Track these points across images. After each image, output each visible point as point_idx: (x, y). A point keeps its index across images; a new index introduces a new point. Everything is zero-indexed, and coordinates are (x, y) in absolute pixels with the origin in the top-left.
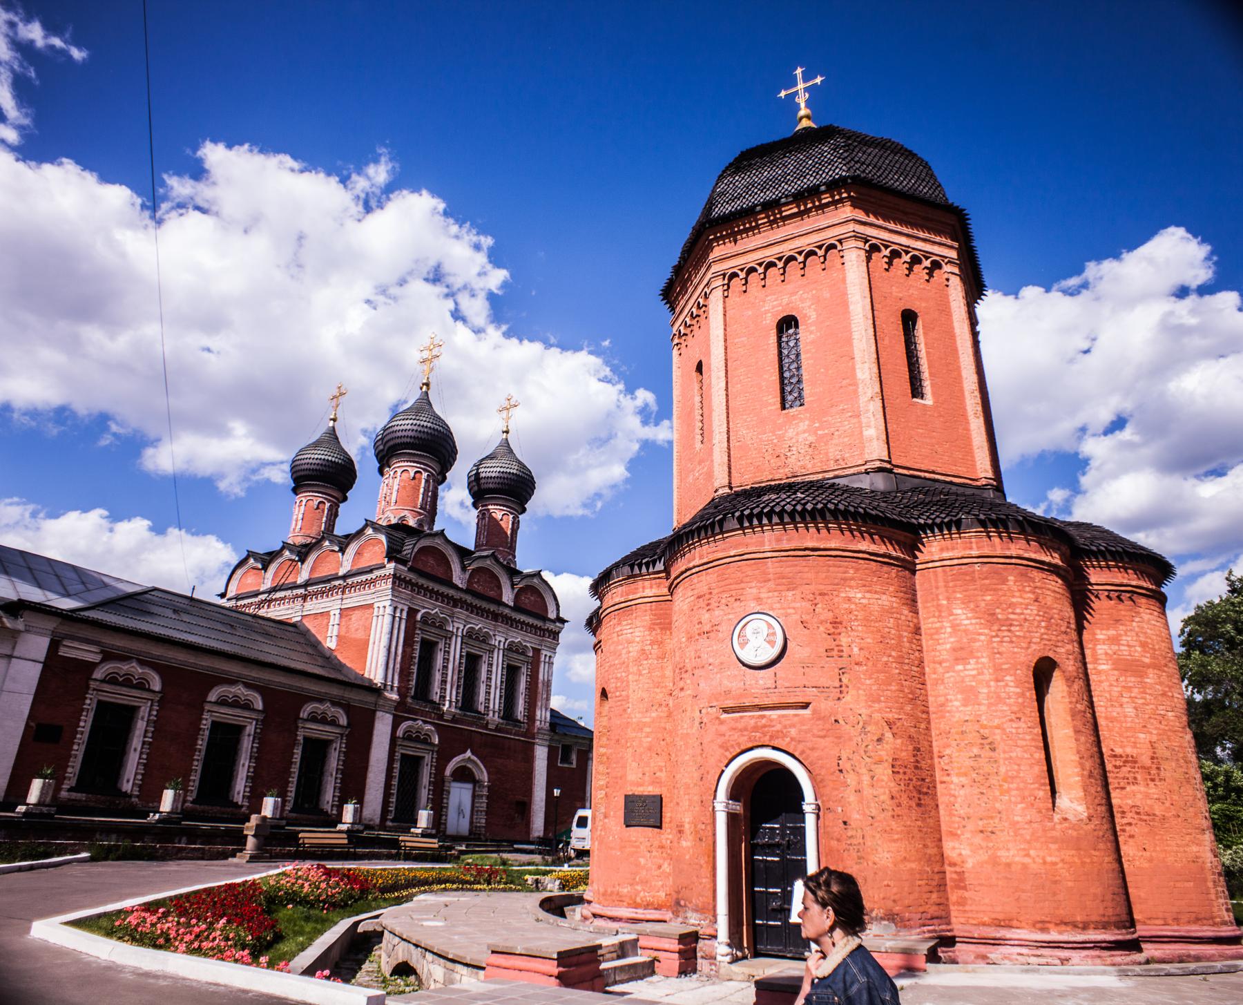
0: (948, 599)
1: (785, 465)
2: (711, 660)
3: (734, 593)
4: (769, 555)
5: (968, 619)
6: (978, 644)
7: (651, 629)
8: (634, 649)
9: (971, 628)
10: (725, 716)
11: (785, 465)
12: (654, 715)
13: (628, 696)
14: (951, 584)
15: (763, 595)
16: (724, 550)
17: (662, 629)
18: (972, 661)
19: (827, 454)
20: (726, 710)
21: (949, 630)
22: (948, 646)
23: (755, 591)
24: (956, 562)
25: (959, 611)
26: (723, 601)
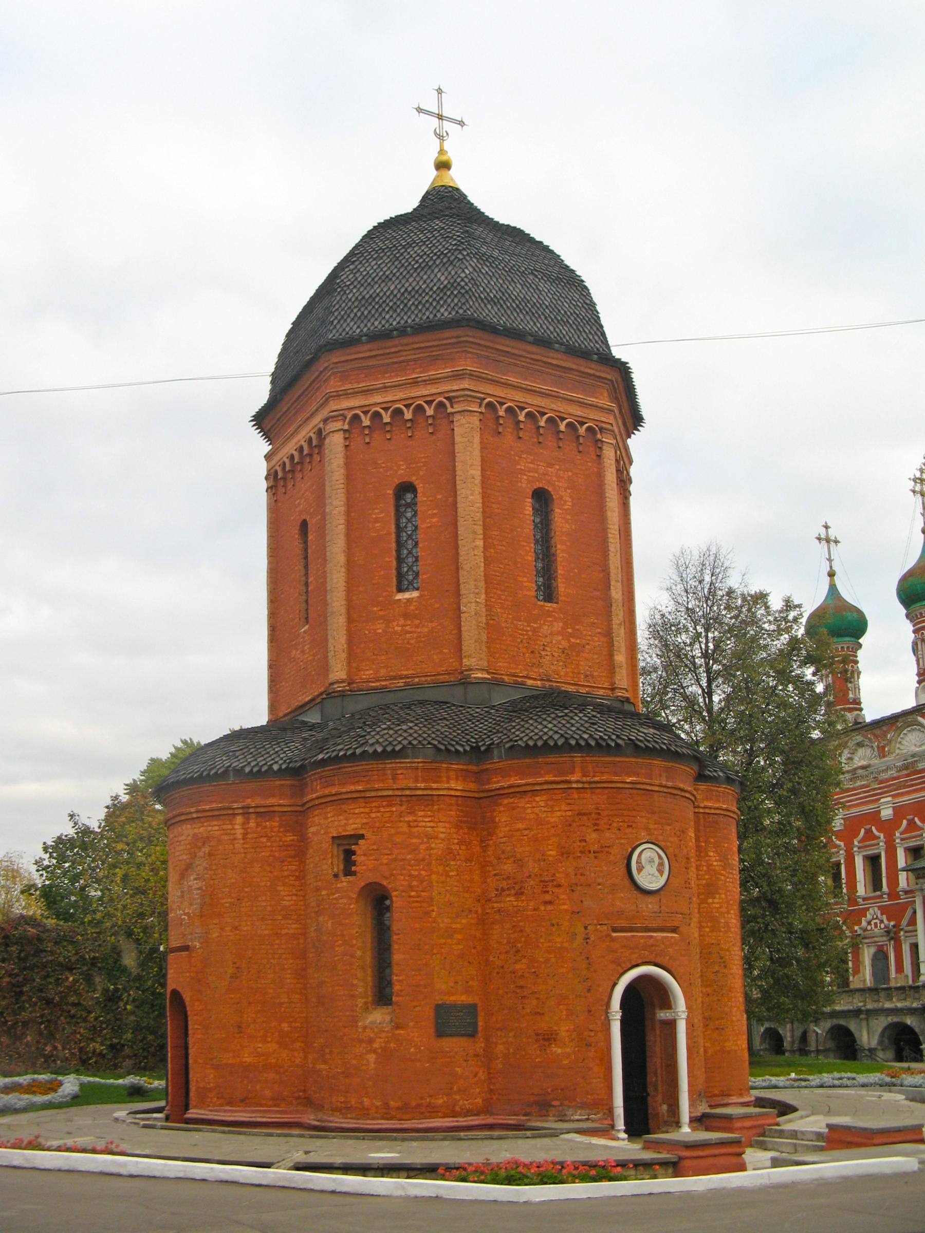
0: (705, 842)
1: (540, 665)
2: (600, 880)
3: (626, 819)
4: (656, 788)
5: (716, 861)
6: (720, 883)
7: (457, 827)
8: (438, 847)
9: (717, 868)
10: (615, 934)
11: (540, 665)
12: (464, 921)
13: (431, 899)
14: (708, 830)
15: (651, 826)
16: (616, 774)
17: (469, 828)
18: (717, 896)
19: (578, 665)
20: (615, 930)
21: (705, 868)
22: (704, 882)
23: (644, 820)
24: (713, 811)
25: (712, 854)
26: (615, 825)
